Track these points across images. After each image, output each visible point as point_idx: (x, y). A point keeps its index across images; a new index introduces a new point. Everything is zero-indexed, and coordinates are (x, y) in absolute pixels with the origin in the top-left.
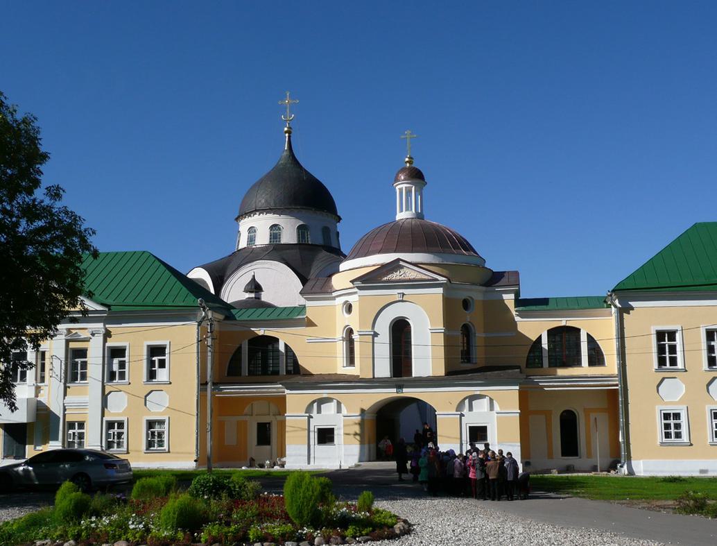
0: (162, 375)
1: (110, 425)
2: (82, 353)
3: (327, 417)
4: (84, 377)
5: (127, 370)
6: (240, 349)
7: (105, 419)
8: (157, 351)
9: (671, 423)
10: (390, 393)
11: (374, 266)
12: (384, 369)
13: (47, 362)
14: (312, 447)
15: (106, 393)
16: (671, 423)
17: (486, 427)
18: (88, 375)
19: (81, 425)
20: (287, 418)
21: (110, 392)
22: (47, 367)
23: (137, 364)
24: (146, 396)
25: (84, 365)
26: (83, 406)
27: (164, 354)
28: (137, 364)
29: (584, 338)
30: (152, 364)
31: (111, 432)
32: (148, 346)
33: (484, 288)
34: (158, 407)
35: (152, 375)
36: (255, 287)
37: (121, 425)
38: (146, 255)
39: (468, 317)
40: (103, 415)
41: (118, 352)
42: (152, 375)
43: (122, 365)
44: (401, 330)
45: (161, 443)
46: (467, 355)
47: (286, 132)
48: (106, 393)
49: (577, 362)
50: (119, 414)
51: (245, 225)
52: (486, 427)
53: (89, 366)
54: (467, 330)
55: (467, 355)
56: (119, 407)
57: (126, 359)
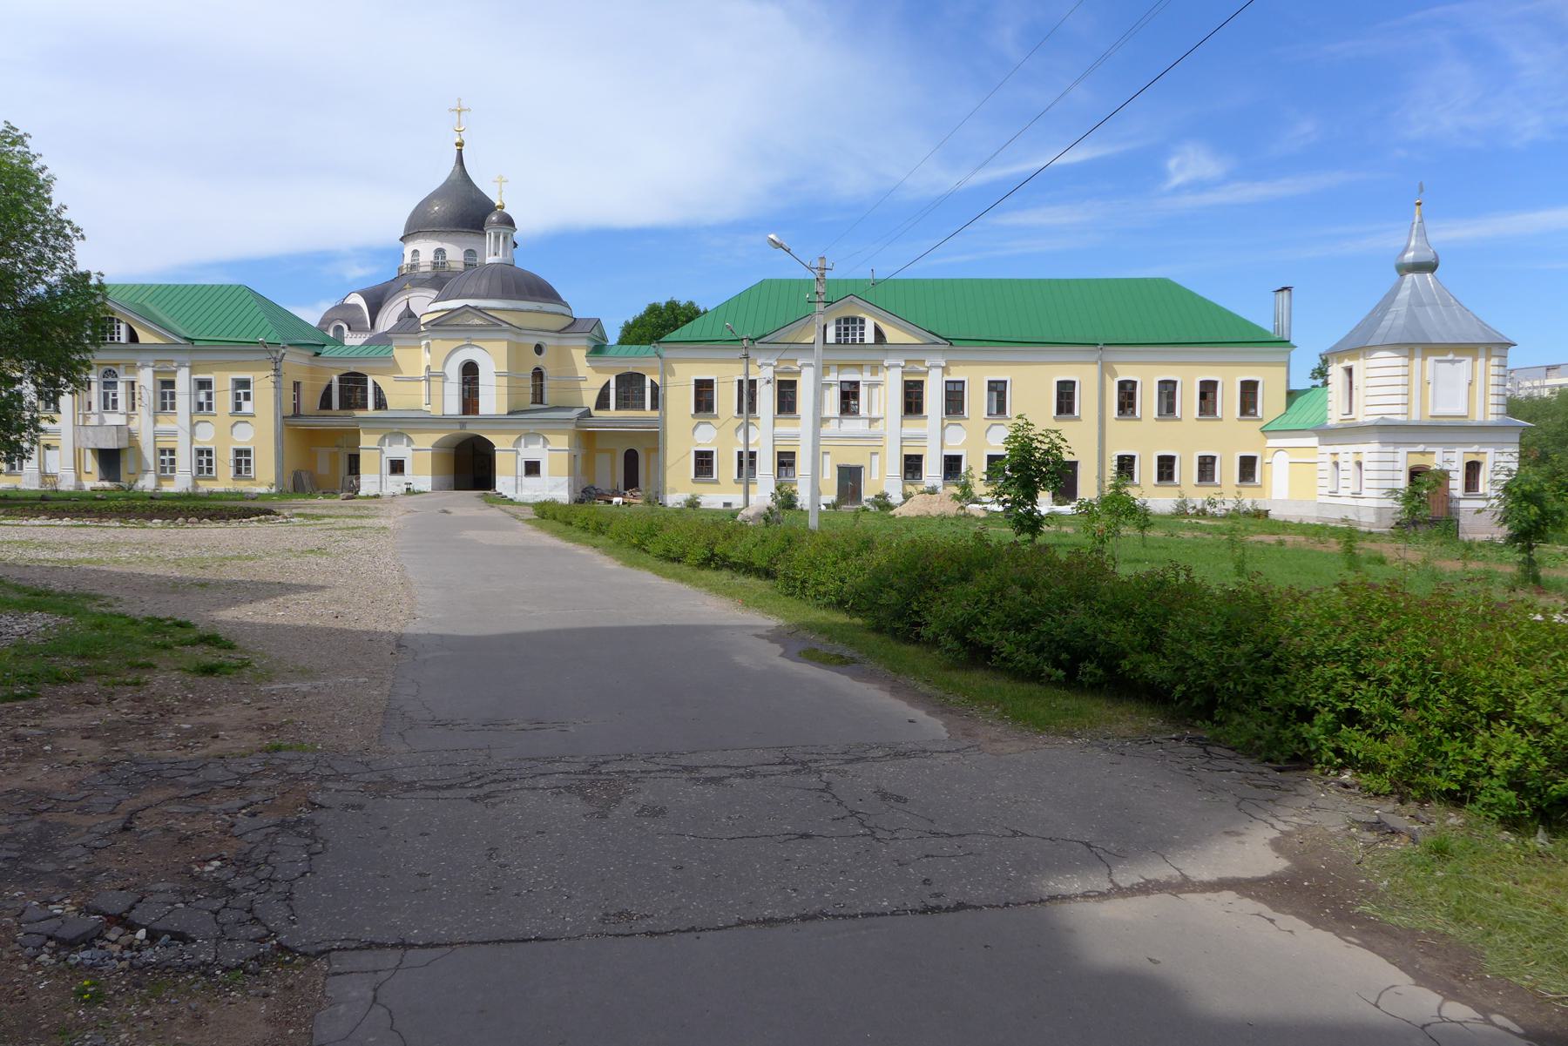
0: (247, 407)
1: (200, 452)
2: (171, 384)
3: (397, 451)
4: (173, 407)
5: (213, 401)
6: (329, 388)
7: (194, 446)
8: (245, 384)
9: (704, 462)
10: (455, 430)
11: (442, 310)
12: (453, 406)
13: (137, 390)
14: (384, 476)
15: (194, 422)
16: (704, 462)
17: (539, 462)
18: (177, 405)
19: (172, 452)
20: (361, 451)
21: (199, 422)
22: (137, 396)
23: (223, 398)
24: (233, 426)
25: (173, 396)
26: (174, 434)
27: (249, 387)
28: (223, 398)
29: (648, 383)
30: (238, 396)
31: (201, 458)
32: (233, 379)
33: (558, 335)
34: (244, 436)
35: (238, 407)
36: (409, 315)
37: (209, 452)
38: (241, 289)
39: (539, 361)
40: (192, 443)
41: (204, 384)
42: (238, 407)
43: (209, 396)
44: (470, 371)
45: (248, 470)
46: (538, 397)
47: (457, 145)
48: (194, 422)
49: (643, 407)
50: (206, 443)
52: (539, 462)
53: (177, 396)
54: (538, 374)
55: (538, 397)
56: (206, 436)
57: (213, 390)
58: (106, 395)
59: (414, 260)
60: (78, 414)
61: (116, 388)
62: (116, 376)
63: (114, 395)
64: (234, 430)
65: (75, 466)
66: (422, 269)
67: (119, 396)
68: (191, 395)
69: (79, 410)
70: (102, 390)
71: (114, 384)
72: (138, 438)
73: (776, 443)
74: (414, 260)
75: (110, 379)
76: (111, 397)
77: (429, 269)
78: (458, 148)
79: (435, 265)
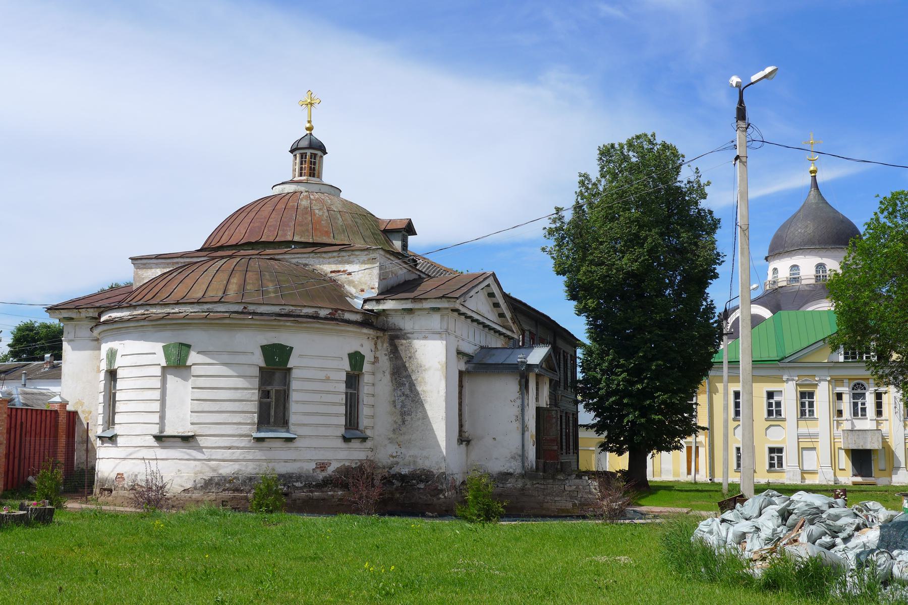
47: (811, 172)
51: (775, 264)
58: (855, 405)
59: (793, 274)
60: (834, 420)
61: (864, 398)
62: (865, 389)
63: (863, 404)
64: (736, 431)
65: (799, 464)
66: (804, 282)
67: (867, 405)
68: (797, 400)
69: (833, 417)
70: (852, 401)
71: (863, 395)
72: (887, 440)
73: (799, 441)
74: (793, 274)
75: (859, 391)
76: (860, 406)
77: (813, 281)
78: (813, 175)
79: (817, 277)
